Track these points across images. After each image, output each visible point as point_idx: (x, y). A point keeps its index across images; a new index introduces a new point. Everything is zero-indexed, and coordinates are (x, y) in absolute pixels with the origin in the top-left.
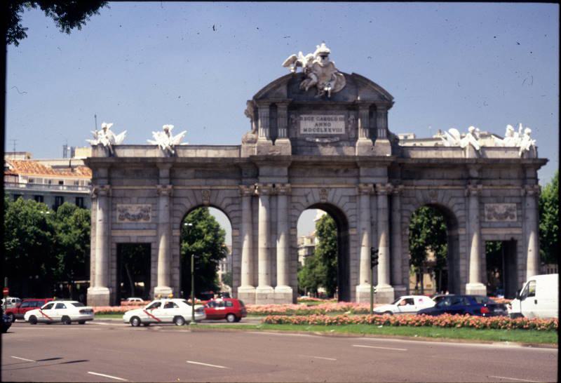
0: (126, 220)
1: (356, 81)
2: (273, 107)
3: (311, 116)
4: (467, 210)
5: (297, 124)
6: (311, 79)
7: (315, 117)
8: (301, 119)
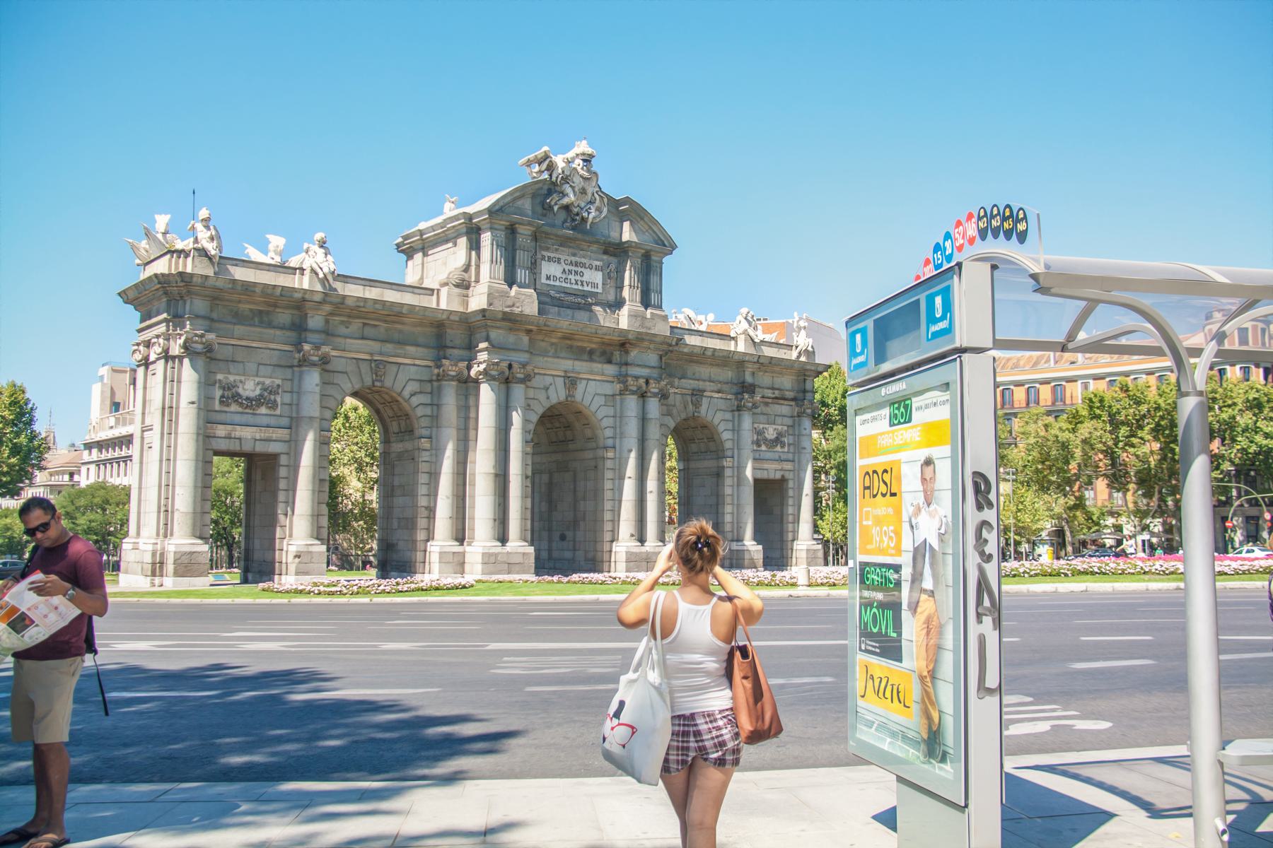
0: (234, 407)
1: (628, 210)
4: (737, 430)
6: (564, 195)
7: (563, 258)
8: (543, 258)
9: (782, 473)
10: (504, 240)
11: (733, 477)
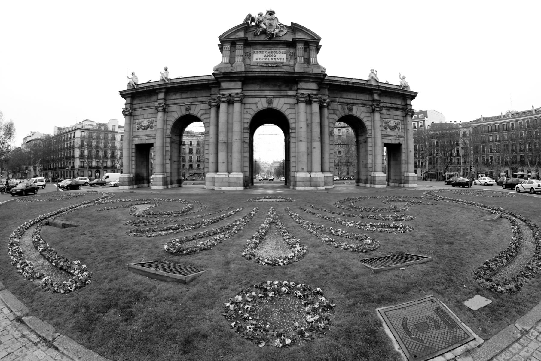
0: (141, 130)
2: (233, 43)
3: (261, 51)
4: (373, 121)
5: (249, 56)
6: (261, 27)
7: (264, 51)
8: (254, 52)
9: (399, 141)
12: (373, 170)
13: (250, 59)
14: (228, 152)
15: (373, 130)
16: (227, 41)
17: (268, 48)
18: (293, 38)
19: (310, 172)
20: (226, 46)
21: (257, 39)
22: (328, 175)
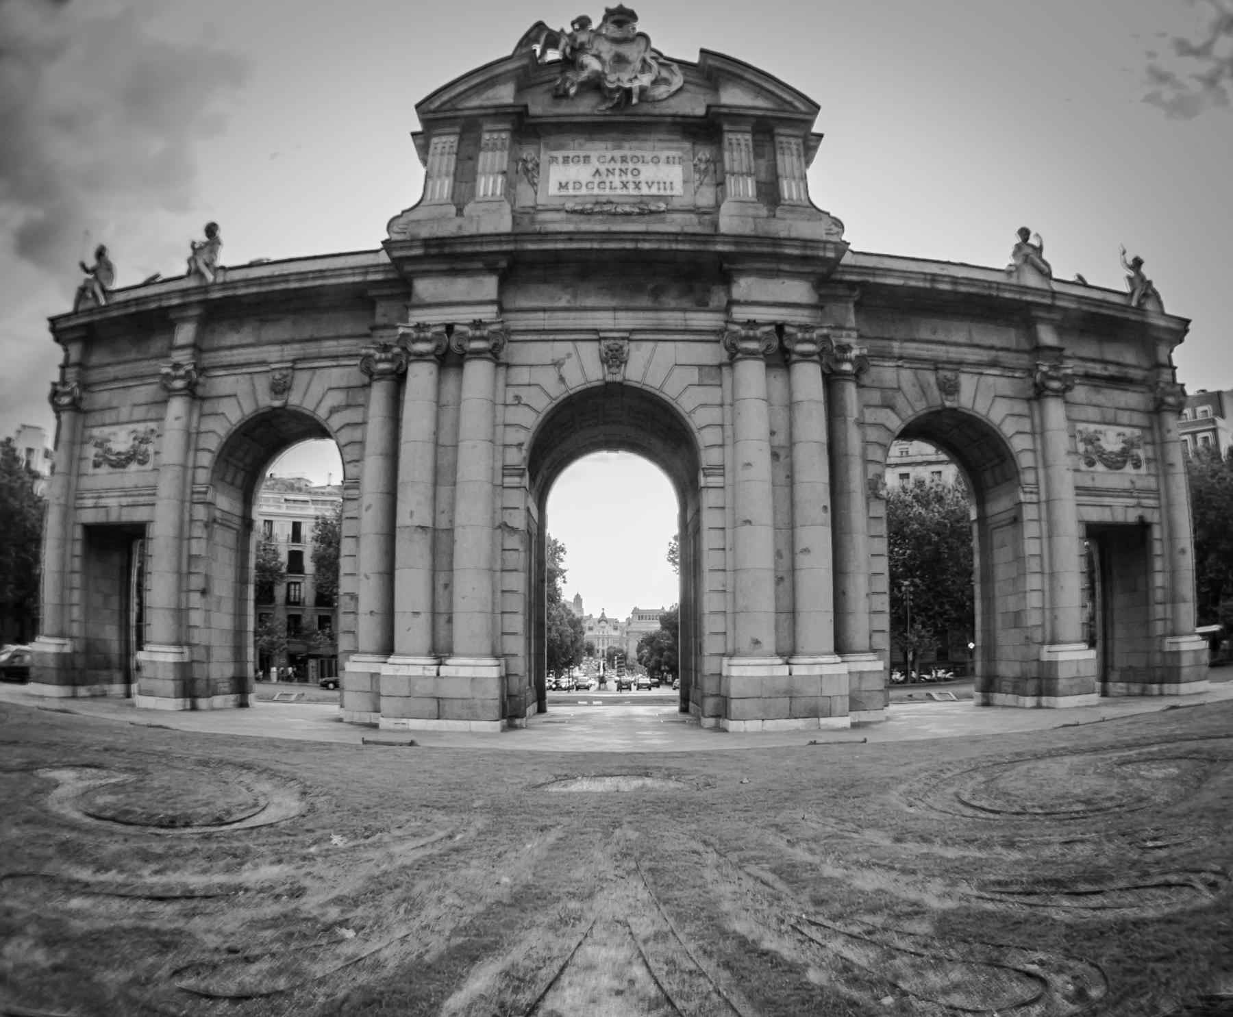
4: (1039, 432)
6: (583, 67)
7: (594, 156)
10: (455, 144)
11: (1039, 520)
12: (1048, 638)
13: (534, 185)
14: (434, 571)
15: (1041, 472)
16: (446, 118)
17: (610, 144)
18: (709, 107)
19: (788, 654)
20: (444, 139)
21: (563, 109)
22: (867, 667)
